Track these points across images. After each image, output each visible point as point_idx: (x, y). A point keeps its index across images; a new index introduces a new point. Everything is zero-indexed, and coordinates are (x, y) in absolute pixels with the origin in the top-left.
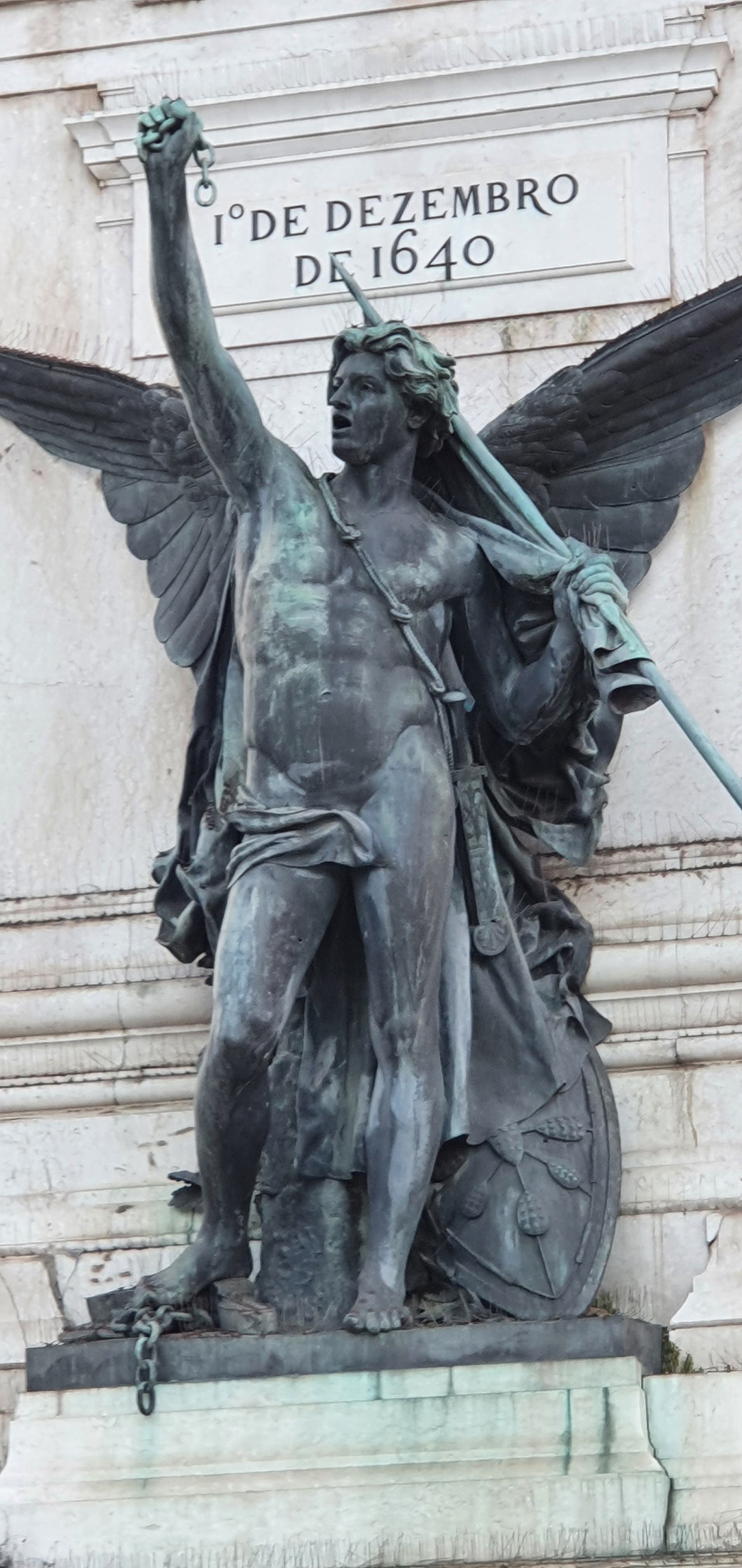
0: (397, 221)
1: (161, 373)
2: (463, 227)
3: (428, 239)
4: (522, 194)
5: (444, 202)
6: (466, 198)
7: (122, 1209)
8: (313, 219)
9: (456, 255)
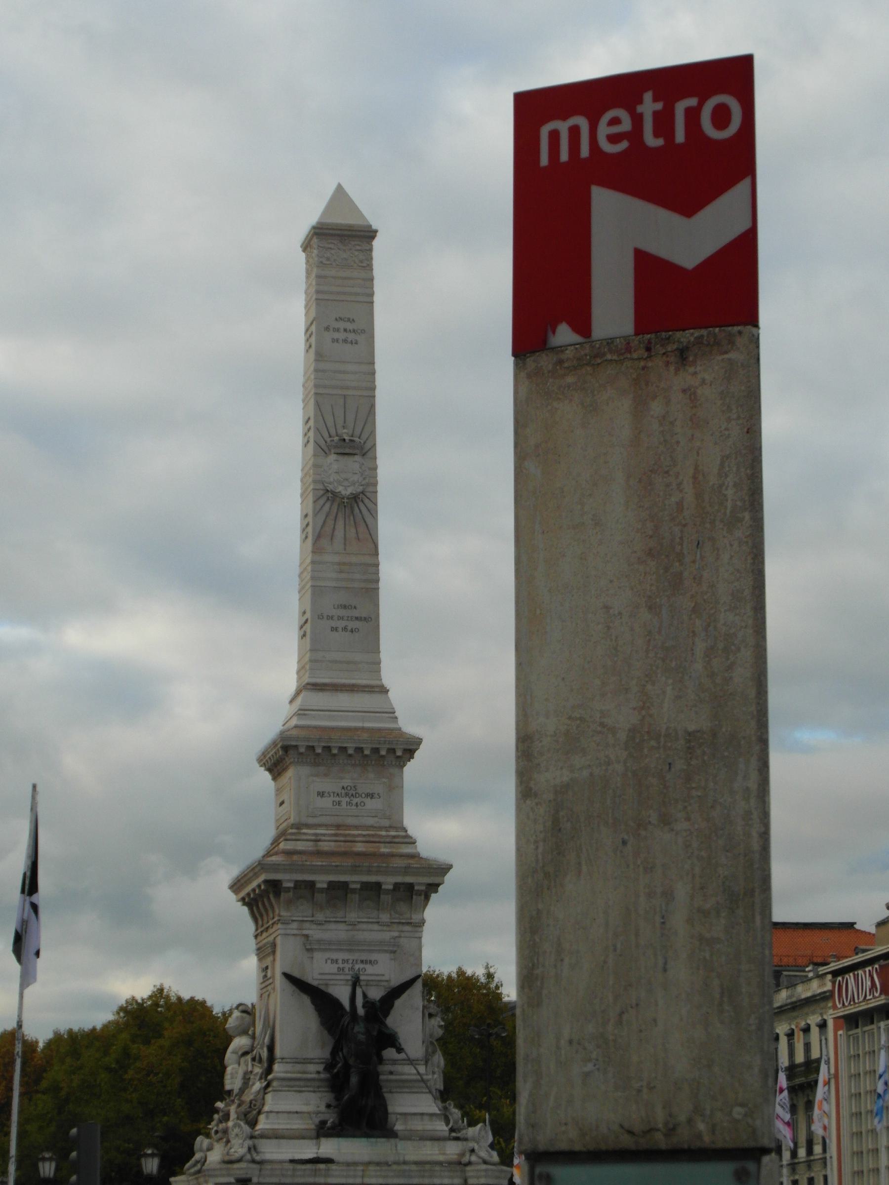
1: (346, 1003)
2: (362, 966)
3: (357, 967)
6: (362, 962)
8: (340, 961)
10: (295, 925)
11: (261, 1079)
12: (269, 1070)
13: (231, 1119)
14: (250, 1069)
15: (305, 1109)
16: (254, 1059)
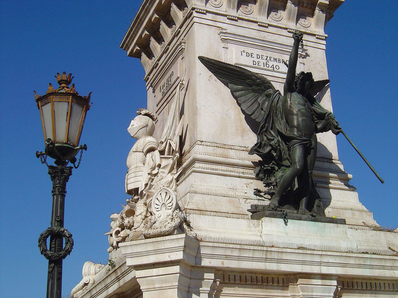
0: (266, 60)
2: (275, 64)
3: (271, 63)
4: (282, 61)
5: (272, 59)
6: (275, 60)
7: (246, 193)
8: (254, 56)
9: (275, 67)
10: (209, 16)
11: (172, 169)
12: (179, 163)
13: (137, 213)
14: (158, 162)
15: (231, 193)
16: (162, 152)
